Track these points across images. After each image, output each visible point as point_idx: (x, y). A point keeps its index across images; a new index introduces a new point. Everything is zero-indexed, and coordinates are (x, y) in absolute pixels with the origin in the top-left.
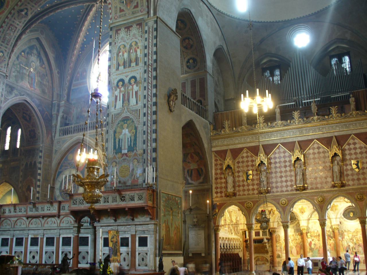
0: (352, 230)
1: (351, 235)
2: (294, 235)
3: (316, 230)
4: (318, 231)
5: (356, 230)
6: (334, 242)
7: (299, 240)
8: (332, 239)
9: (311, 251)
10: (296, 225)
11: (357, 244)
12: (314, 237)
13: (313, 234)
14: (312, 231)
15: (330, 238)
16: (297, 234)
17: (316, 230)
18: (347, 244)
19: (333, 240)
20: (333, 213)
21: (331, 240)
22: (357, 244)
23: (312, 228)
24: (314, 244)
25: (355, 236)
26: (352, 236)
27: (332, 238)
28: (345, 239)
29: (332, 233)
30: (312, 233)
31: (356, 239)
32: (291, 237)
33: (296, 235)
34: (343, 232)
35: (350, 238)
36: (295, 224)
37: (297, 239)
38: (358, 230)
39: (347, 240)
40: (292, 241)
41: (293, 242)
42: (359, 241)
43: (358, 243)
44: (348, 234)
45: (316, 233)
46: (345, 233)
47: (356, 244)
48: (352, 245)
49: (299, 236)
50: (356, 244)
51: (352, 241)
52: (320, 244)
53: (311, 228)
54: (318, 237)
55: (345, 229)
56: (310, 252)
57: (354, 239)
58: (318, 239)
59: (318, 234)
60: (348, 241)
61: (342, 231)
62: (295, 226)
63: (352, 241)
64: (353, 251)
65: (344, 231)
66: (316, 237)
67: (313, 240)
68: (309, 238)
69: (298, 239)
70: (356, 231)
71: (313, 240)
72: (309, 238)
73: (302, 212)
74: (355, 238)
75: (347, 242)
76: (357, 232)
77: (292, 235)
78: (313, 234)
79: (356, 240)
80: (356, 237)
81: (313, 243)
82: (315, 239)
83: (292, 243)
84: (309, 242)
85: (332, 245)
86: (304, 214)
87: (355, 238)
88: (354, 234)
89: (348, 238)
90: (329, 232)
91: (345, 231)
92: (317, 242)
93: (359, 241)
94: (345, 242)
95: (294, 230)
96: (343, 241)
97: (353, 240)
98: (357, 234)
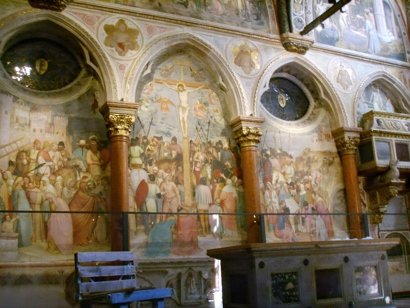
0: (295, 153)
1: (290, 170)
2: (68, 147)
3: (168, 134)
4: (175, 139)
5: (305, 154)
6: (235, 195)
7: (88, 171)
8: (229, 181)
9: (142, 227)
10: (80, 99)
11: (310, 206)
12: (159, 163)
13: (155, 151)
14: (150, 137)
15: (223, 175)
16: (83, 142)
17: (168, 134)
18: (280, 204)
19: (234, 185)
20: (244, 75)
21: (223, 182)
22: (310, 206)
23: (151, 123)
24: (159, 196)
25: (303, 174)
26: (296, 173)
27: (228, 175)
28: (274, 182)
29: (229, 154)
30: (149, 147)
31: (308, 186)
32: (51, 154)
33: (74, 148)
34: (267, 155)
35: (289, 182)
36: (75, 96)
37: (77, 166)
38: (311, 155)
39: (278, 186)
40: (54, 173)
41: (59, 178)
42: (315, 193)
43: (313, 201)
44: (282, 166)
45: (170, 149)
46: (275, 162)
47: (306, 204)
48: (293, 207)
49: (89, 153)
50: (306, 204)
51: (294, 192)
52: (183, 200)
53: (146, 127)
54: (173, 166)
55: (273, 147)
56: (136, 233)
57: (302, 186)
58: (173, 173)
59: (174, 154)
60: (282, 192)
61: (263, 151)
62: (76, 106)
63: (294, 192)
64: (297, 231)
65: (268, 152)
66: (166, 165)
67: (152, 178)
68: (136, 166)
69: (84, 169)
70: (305, 157)
71: (152, 178)
72: (136, 166)
73: (121, 45)
74: (306, 182)
75: (278, 194)
76: (309, 162)
77: (56, 146)
78: (155, 151)
79: (307, 189)
80: (306, 177)
81: (153, 189)
82: (162, 171)
83: (54, 183)
84: (136, 184)
85: (229, 206)
86: (130, 54)
87: (306, 182)
88: (301, 169)
89: (281, 179)
90: (218, 150)
91: (273, 151)
92: (170, 185)
93: (315, 193)
94: (274, 193)
95: (70, 120)
96: (267, 193)
97: (298, 190)
98: (310, 167)
